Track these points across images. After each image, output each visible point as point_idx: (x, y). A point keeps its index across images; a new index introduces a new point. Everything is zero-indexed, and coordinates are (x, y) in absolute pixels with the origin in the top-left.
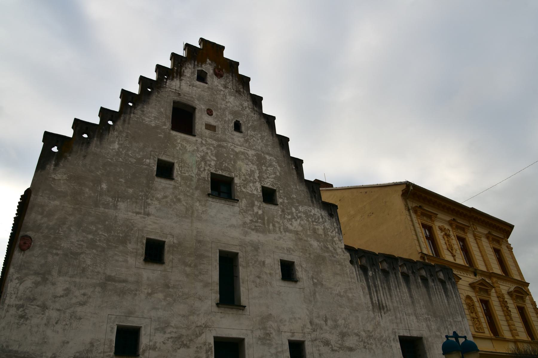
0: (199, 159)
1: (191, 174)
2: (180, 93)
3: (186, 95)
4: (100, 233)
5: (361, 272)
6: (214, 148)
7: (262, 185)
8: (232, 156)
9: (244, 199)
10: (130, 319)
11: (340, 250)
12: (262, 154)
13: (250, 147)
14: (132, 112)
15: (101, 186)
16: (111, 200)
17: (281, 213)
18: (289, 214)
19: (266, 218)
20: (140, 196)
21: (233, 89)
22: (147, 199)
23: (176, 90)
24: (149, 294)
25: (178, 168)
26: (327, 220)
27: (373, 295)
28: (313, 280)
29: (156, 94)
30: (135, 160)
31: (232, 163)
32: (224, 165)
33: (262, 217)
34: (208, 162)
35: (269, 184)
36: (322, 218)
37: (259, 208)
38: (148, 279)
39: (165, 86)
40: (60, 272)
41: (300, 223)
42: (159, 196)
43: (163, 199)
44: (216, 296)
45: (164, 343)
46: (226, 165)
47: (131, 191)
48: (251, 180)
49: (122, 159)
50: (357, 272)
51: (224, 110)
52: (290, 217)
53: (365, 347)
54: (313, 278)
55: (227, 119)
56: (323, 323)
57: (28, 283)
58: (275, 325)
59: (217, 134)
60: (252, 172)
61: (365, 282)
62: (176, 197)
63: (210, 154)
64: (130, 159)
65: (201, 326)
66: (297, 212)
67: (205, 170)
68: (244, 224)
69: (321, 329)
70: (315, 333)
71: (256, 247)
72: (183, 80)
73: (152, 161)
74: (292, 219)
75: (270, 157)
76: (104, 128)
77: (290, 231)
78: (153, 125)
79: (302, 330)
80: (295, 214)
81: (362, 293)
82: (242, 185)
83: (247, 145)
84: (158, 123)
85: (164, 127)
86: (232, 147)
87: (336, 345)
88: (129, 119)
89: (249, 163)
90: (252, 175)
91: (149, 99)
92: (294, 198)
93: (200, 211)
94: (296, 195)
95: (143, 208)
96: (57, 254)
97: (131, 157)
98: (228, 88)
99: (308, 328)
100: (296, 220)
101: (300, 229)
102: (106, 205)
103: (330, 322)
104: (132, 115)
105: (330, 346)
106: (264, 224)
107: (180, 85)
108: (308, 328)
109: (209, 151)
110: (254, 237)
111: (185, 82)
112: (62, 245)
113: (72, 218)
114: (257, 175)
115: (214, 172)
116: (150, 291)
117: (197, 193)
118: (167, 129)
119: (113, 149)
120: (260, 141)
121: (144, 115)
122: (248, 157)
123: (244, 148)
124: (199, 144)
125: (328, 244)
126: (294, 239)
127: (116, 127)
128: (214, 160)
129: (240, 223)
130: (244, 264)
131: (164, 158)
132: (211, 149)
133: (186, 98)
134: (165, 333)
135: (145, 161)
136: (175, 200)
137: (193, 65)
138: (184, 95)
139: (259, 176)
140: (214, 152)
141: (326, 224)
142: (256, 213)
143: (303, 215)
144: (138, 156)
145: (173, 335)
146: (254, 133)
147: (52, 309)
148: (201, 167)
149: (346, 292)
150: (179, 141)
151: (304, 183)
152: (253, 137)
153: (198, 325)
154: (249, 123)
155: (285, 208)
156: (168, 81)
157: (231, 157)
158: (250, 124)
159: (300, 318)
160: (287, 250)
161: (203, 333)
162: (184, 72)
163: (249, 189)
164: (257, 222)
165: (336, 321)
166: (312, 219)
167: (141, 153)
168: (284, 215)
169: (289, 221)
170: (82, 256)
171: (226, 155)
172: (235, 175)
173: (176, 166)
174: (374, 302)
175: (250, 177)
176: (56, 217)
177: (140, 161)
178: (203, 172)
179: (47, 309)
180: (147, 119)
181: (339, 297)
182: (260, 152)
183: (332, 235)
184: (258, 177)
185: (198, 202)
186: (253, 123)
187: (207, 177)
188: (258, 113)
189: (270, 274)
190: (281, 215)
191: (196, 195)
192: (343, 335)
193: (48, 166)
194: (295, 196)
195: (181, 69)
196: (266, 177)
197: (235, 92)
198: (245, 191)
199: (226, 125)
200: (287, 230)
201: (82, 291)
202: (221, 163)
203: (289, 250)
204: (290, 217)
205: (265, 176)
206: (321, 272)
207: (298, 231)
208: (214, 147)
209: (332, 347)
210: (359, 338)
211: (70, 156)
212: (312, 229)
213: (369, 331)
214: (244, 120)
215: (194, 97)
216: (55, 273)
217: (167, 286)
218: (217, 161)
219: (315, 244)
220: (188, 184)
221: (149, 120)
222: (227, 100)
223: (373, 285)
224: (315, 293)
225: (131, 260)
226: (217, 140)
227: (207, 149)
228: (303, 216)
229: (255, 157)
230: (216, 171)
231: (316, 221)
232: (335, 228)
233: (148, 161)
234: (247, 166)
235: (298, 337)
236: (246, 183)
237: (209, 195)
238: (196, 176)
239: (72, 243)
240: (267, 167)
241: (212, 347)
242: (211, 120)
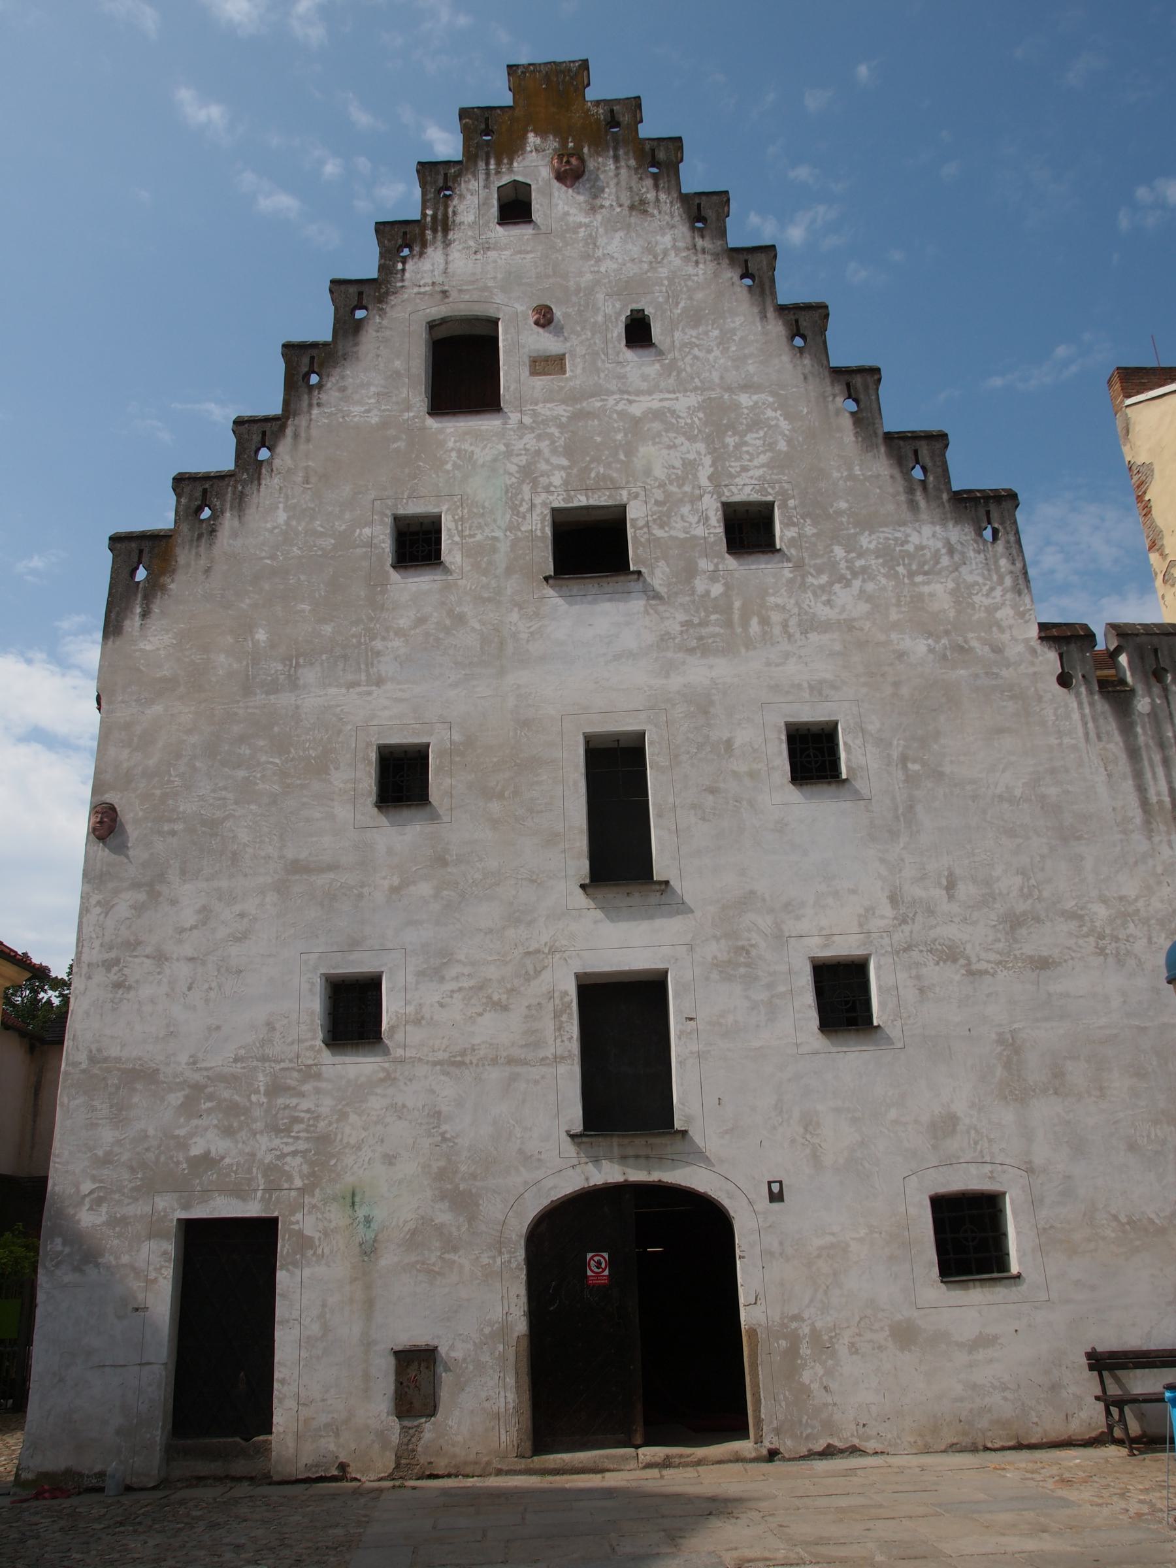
0: (514, 480)
1: (493, 531)
2: (446, 288)
3: (465, 288)
4: (263, 759)
5: (1102, 706)
6: (560, 430)
7: (724, 499)
8: (619, 437)
9: (662, 563)
10: (355, 956)
11: (1020, 648)
12: (726, 396)
13: (683, 387)
14: (315, 402)
15: (252, 640)
16: (280, 667)
17: (791, 575)
18: (820, 571)
19: (737, 604)
20: (353, 636)
21: (621, 206)
22: (373, 639)
23: (433, 284)
24: (394, 890)
25: (452, 525)
26: (972, 554)
27: (1149, 775)
28: (905, 768)
29: (378, 319)
30: (333, 541)
31: (622, 457)
32: (593, 475)
33: (723, 607)
34: (544, 481)
35: (748, 489)
36: (951, 551)
37: (713, 577)
39: (399, 284)
40: (183, 872)
41: (862, 591)
42: (403, 622)
43: (415, 628)
44: (582, 867)
45: (442, 1005)
46: (602, 470)
47: (328, 629)
48: (686, 493)
49: (300, 548)
50: (1087, 711)
53: (1101, 951)
54: (904, 759)
55: (600, 318)
56: (939, 893)
57: (122, 909)
58: (765, 922)
59: (570, 379)
60: (690, 466)
61: (1117, 737)
62: (450, 612)
63: (546, 452)
64: (319, 542)
65: (538, 951)
66: (853, 555)
67: (533, 506)
68: (662, 640)
69: (931, 912)
70: (906, 928)
72: (454, 241)
73: (378, 528)
74: (831, 584)
75: (755, 397)
76: (245, 476)
77: (825, 627)
79: (861, 925)
80: (843, 565)
81: (1101, 777)
82: (654, 520)
83: (671, 381)
84: (388, 410)
86: (620, 407)
87: (983, 955)
88: (308, 427)
89: (681, 439)
90: (690, 476)
91: (356, 344)
92: (840, 513)
93: (524, 636)
94: (847, 501)
95: (363, 666)
96: (173, 833)
97: (322, 535)
98: (602, 207)
99: (883, 917)
100: (848, 584)
101: (864, 607)
102: (273, 688)
103: (965, 890)
104: (315, 411)
105: (962, 961)
107: (447, 263)
108: (883, 917)
109: (544, 445)
111: (460, 247)
112: (181, 809)
113: (194, 739)
115: (563, 505)
116: (396, 881)
117: (512, 585)
118: (414, 417)
119: (275, 528)
120: (717, 352)
122: (674, 421)
123: (662, 396)
124: (512, 433)
125: (970, 635)
126: (838, 647)
127: (277, 462)
128: (563, 468)
132: (550, 436)
133: (467, 297)
134: (442, 979)
135: (360, 534)
136: (448, 622)
137: (482, 177)
138: (460, 291)
139: (712, 474)
140: (561, 442)
141: (964, 570)
142: (702, 596)
143: (873, 562)
144: (341, 526)
145: (466, 983)
146: (694, 333)
147: (178, 960)
148: (523, 500)
150: (450, 444)
151: (883, 449)
152: (691, 348)
153: (531, 950)
154: (677, 304)
155: (805, 555)
156: (409, 266)
157: (616, 441)
158: (682, 304)
159: (853, 892)
160: (811, 688)
161: (545, 968)
162: (454, 213)
163: (680, 525)
164: (704, 623)
166: (910, 564)
167: (347, 516)
168: (803, 577)
169: (819, 592)
170: (228, 824)
171: (599, 439)
172: (629, 494)
174: (1154, 799)
175: (680, 486)
178: (528, 516)
179: (167, 959)
181: (1006, 805)
182: (718, 390)
183: (987, 602)
184: (710, 478)
185: (516, 609)
186: (690, 298)
187: (539, 526)
188: (708, 257)
190: (791, 581)
191: (509, 591)
192: (1014, 923)
193: (127, 623)
194: (843, 505)
195: (446, 207)
196: (738, 469)
197: (626, 212)
198: (666, 535)
199: (598, 339)
200: (810, 625)
201: (237, 908)
202: (587, 470)
203: (817, 689)
204: (824, 579)
205: (734, 466)
207: (854, 620)
208: (561, 426)
209: (969, 964)
210: (1081, 926)
211: (173, 581)
212: (908, 599)
213: (1121, 898)
214: (661, 300)
215: (491, 284)
218: (570, 467)
219: (919, 647)
220: (484, 565)
221: (363, 409)
222: (599, 253)
223: (1151, 743)
224: (911, 808)
225: (343, 812)
226: (573, 398)
227: (539, 438)
228: (873, 562)
229: (701, 415)
230: (569, 499)
231: (926, 568)
232: (1001, 581)
233: (367, 531)
234: (672, 452)
235: (844, 948)
237: (546, 579)
238: (508, 533)
239: (202, 798)
240: (742, 435)
241: (572, 1001)
242: (545, 342)
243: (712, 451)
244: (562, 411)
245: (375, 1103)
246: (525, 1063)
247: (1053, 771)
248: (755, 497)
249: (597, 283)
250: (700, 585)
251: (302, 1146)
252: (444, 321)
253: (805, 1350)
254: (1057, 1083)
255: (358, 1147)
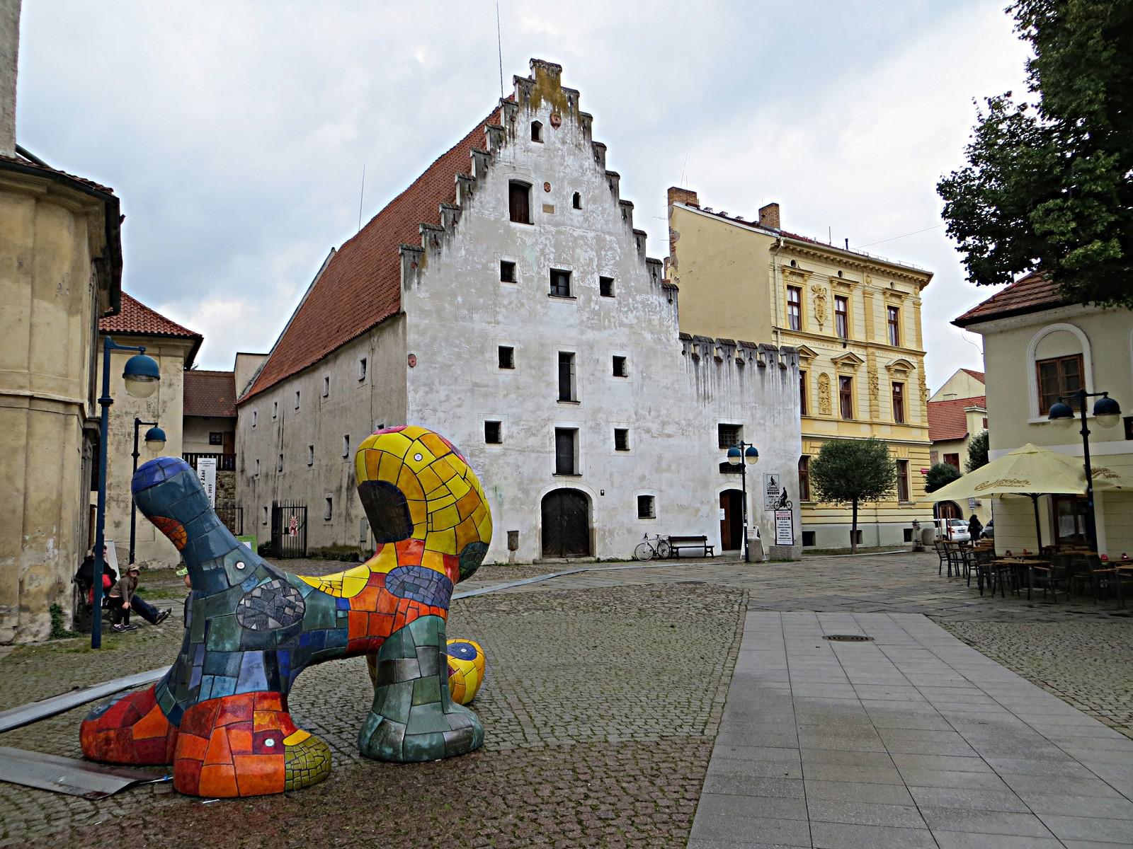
5: (692, 362)
13: (589, 228)
24: (506, 396)
33: (597, 313)
36: (660, 306)
37: (596, 304)
38: (504, 382)
40: (440, 382)
42: (506, 302)
43: (508, 305)
44: (557, 394)
51: (562, 180)
52: (626, 309)
53: (683, 434)
54: (642, 372)
57: (421, 393)
58: (604, 417)
60: (591, 260)
62: (520, 302)
69: (644, 418)
71: (591, 346)
74: (628, 311)
78: (493, 219)
85: (503, 219)
86: (571, 232)
96: (435, 368)
101: (636, 321)
102: (464, 319)
104: (472, 210)
106: (600, 320)
109: (548, 242)
110: (590, 335)
113: (440, 335)
114: (595, 263)
117: (539, 295)
121: (482, 207)
127: (460, 229)
128: (553, 253)
129: (578, 321)
130: (580, 363)
131: (507, 259)
145: (525, 427)
149: (673, 384)
164: (593, 319)
165: (659, 411)
167: (486, 257)
170: (453, 367)
173: (518, 267)
176: (429, 335)
177: (486, 267)
180: (486, 212)
189: (603, 371)
192: (664, 424)
193: (412, 286)
194: (633, 284)
200: (622, 324)
201: (458, 396)
202: (560, 255)
203: (622, 346)
204: (626, 309)
205: (604, 263)
206: (651, 365)
208: (552, 235)
216: (437, 383)
217: (518, 388)
219: (648, 336)
222: (565, 164)
224: (642, 387)
226: (557, 225)
228: (640, 306)
236: (584, 274)
237: (549, 295)
242: (548, 199)
243: (598, 256)
244: (553, 229)
245: (501, 461)
246: (541, 452)
247: (678, 381)
248: (609, 276)
249: (565, 177)
250: (593, 305)
251: (480, 473)
252: (514, 180)
253: (607, 534)
254: (668, 469)
255: (497, 474)
